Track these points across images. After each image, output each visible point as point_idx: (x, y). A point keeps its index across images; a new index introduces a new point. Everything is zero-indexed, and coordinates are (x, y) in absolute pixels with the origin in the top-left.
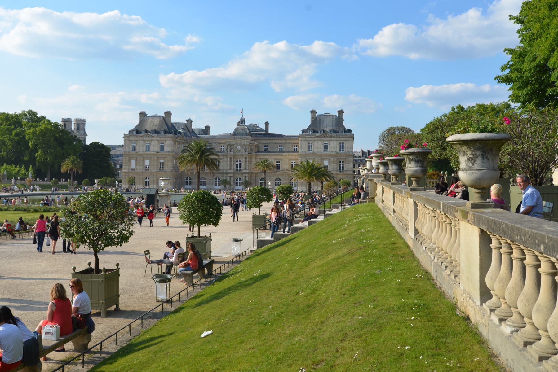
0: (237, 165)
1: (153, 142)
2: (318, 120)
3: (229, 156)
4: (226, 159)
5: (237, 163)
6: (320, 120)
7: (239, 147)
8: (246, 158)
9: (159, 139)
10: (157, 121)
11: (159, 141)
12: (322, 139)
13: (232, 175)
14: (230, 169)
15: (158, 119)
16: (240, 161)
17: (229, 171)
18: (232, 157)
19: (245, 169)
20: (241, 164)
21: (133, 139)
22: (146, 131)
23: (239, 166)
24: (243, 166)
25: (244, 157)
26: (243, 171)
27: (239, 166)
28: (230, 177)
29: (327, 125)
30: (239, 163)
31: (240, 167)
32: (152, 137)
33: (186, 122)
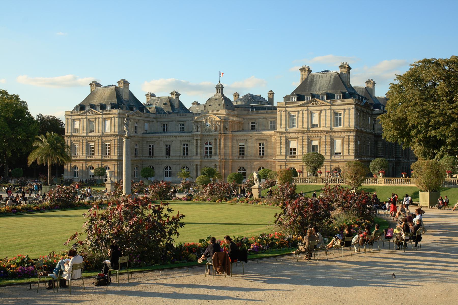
0: (206, 148)
2: (309, 81)
5: (206, 146)
6: (312, 81)
8: (216, 139)
9: (104, 116)
12: (309, 108)
13: (199, 163)
14: (197, 154)
16: (210, 144)
17: (194, 158)
18: (199, 138)
19: (216, 154)
20: (211, 149)
22: (93, 106)
23: (208, 150)
24: (213, 150)
27: (208, 150)
28: (197, 165)
29: (320, 88)
30: (209, 146)
31: (211, 152)
32: (97, 114)
33: (170, 96)
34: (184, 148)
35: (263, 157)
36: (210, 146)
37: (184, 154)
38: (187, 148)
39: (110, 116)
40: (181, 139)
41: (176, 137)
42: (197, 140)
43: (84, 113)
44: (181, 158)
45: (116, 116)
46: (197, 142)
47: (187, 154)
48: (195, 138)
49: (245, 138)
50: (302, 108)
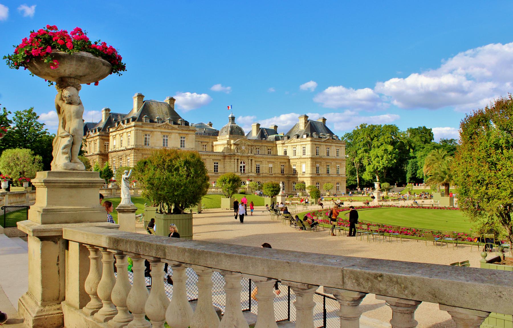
0: (241, 167)
1: (173, 136)
3: (236, 158)
4: (227, 160)
7: (243, 148)
8: (251, 160)
9: (180, 132)
10: (165, 109)
11: (179, 134)
15: (164, 105)
16: (244, 163)
20: (244, 167)
21: (147, 129)
23: (243, 168)
25: (250, 158)
26: (247, 175)
27: (243, 168)
31: (244, 170)
32: (173, 129)
34: (215, 166)
35: (272, 175)
36: (244, 165)
37: (215, 171)
38: (217, 166)
39: (187, 132)
40: (214, 157)
41: (210, 156)
42: (238, 159)
43: (159, 126)
44: (214, 174)
45: (193, 132)
46: (238, 161)
47: (217, 171)
48: (236, 158)
49: (261, 160)
50: (323, 143)
